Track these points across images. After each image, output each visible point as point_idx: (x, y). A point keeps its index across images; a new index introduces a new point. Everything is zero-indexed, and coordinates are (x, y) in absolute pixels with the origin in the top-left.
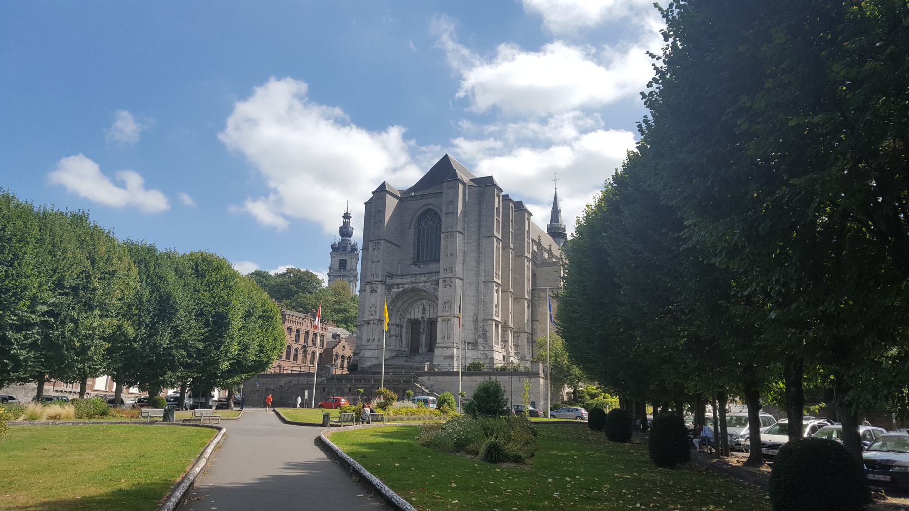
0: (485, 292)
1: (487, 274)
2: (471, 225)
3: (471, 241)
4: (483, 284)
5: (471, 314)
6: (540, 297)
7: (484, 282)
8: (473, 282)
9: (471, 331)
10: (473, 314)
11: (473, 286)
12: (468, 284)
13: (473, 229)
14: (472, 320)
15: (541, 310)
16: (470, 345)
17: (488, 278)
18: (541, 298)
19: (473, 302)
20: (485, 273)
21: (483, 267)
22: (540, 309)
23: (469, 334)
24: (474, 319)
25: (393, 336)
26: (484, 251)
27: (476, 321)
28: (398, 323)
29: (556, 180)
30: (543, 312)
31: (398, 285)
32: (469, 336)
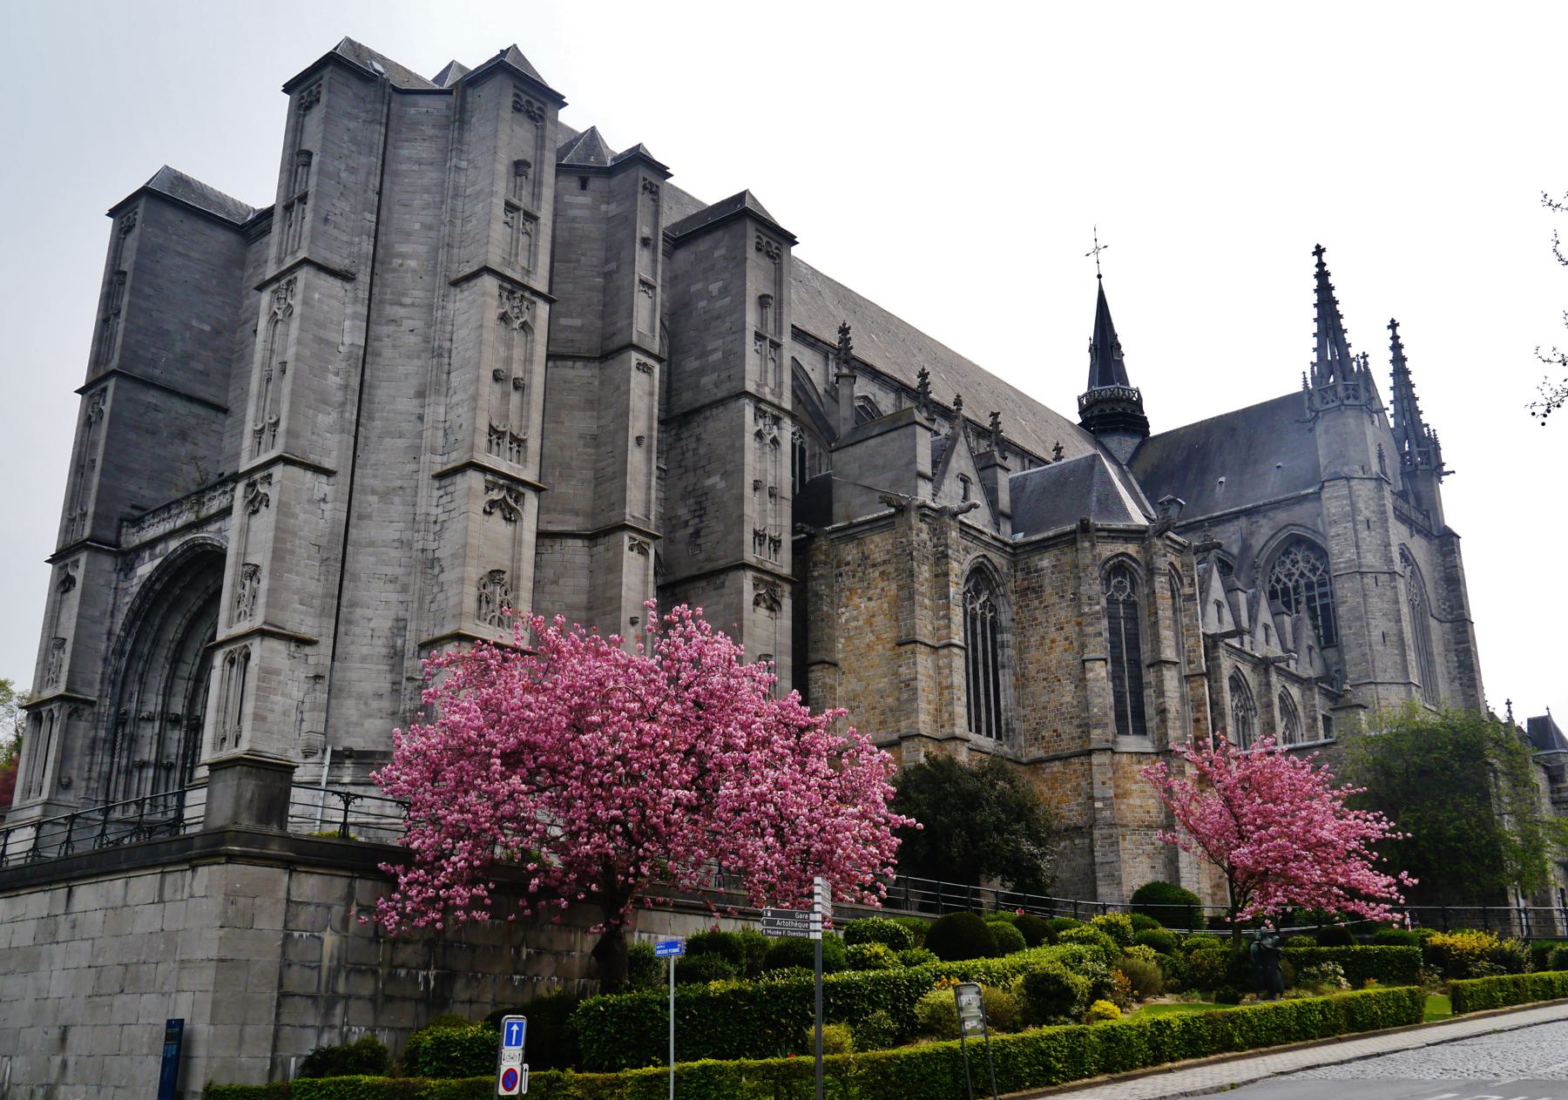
0: (441, 518)
1: (452, 439)
2: (404, 248)
3: (402, 311)
4: (437, 484)
5: (383, 623)
6: (838, 567)
7: (440, 476)
8: (399, 483)
9: (375, 704)
10: (390, 624)
11: (397, 500)
12: (374, 492)
13: (412, 263)
14: (384, 651)
15: (843, 619)
16: (348, 763)
17: (454, 455)
18: (844, 569)
19: (399, 571)
20: (446, 435)
21: (442, 410)
22: (840, 617)
23: (370, 716)
24: (394, 647)
25: (143, 765)
26: (447, 344)
27: (396, 656)
28: (178, 707)
29: (1097, 250)
30: (853, 624)
31: (151, 544)
32: (368, 723)
